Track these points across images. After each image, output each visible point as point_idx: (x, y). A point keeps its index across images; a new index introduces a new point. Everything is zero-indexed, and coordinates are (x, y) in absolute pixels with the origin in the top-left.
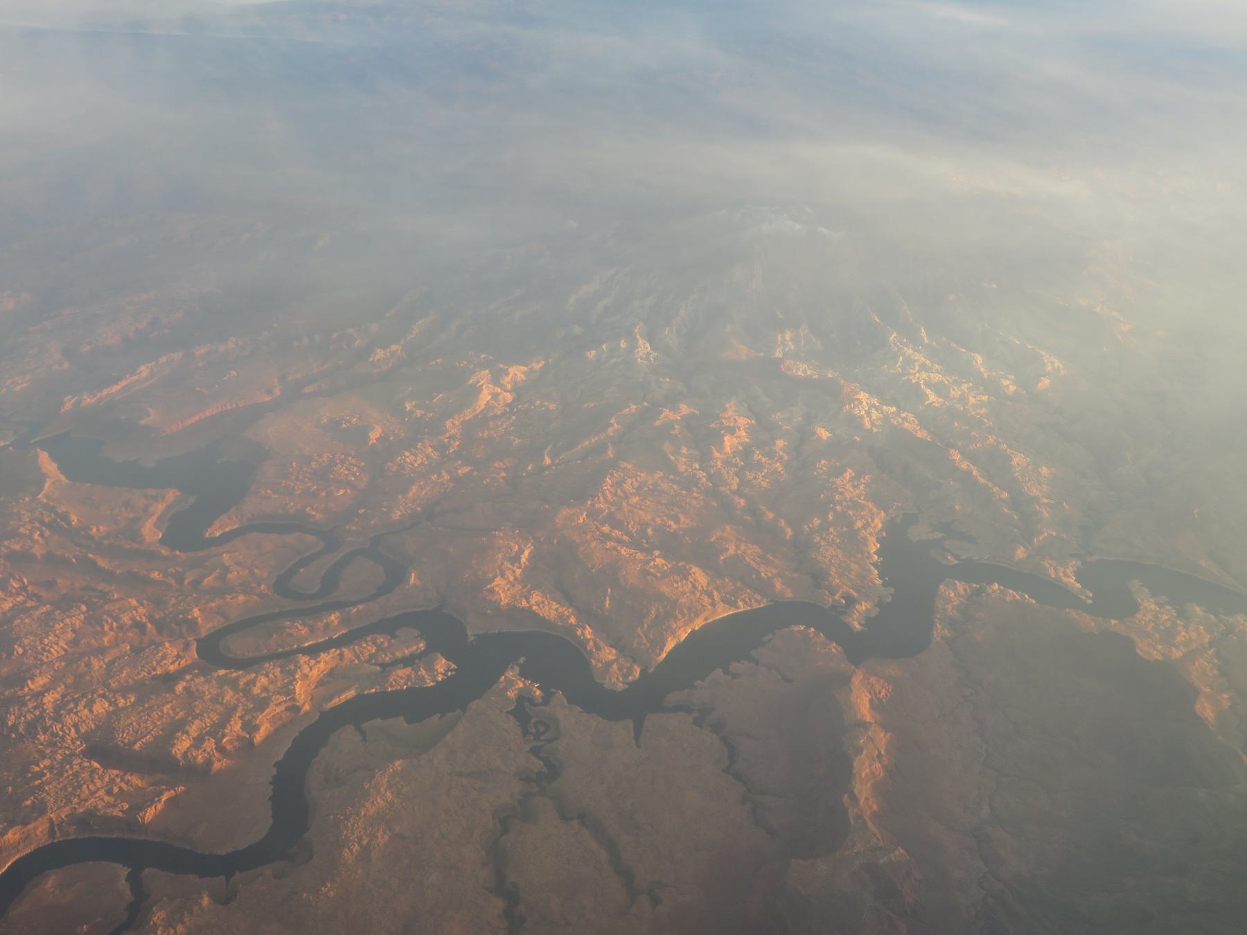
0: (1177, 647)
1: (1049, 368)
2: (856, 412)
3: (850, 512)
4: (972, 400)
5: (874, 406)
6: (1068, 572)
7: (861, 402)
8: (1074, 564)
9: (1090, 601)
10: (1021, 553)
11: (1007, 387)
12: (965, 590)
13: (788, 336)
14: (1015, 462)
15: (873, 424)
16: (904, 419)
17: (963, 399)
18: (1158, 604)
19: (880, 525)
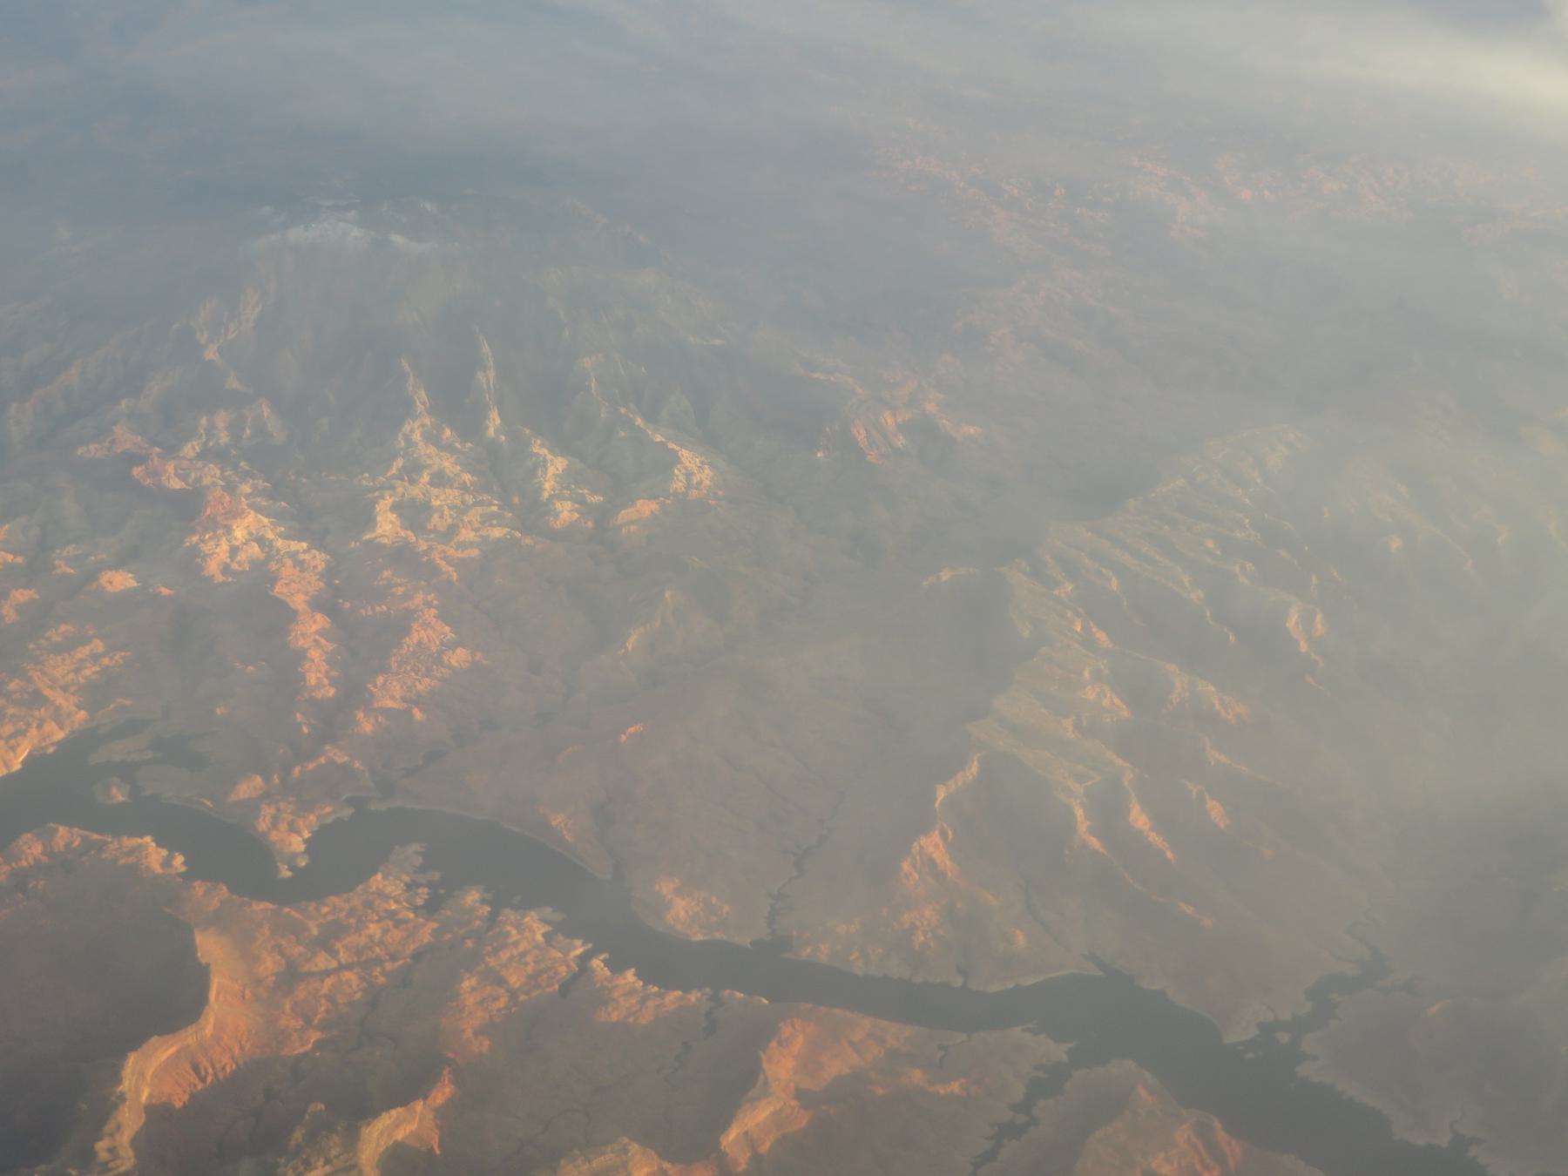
0: (333, 953)
1: (678, 485)
2: (205, 548)
3: (11, 711)
4: (467, 535)
5: (261, 540)
6: (301, 823)
7: (229, 530)
8: (328, 811)
9: (289, 874)
10: (249, 787)
11: (557, 516)
12: (67, 846)
13: (222, 418)
14: (418, 635)
15: (226, 570)
16: (300, 565)
17: (452, 530)
18: (411, 887)
19: (60, 735)
